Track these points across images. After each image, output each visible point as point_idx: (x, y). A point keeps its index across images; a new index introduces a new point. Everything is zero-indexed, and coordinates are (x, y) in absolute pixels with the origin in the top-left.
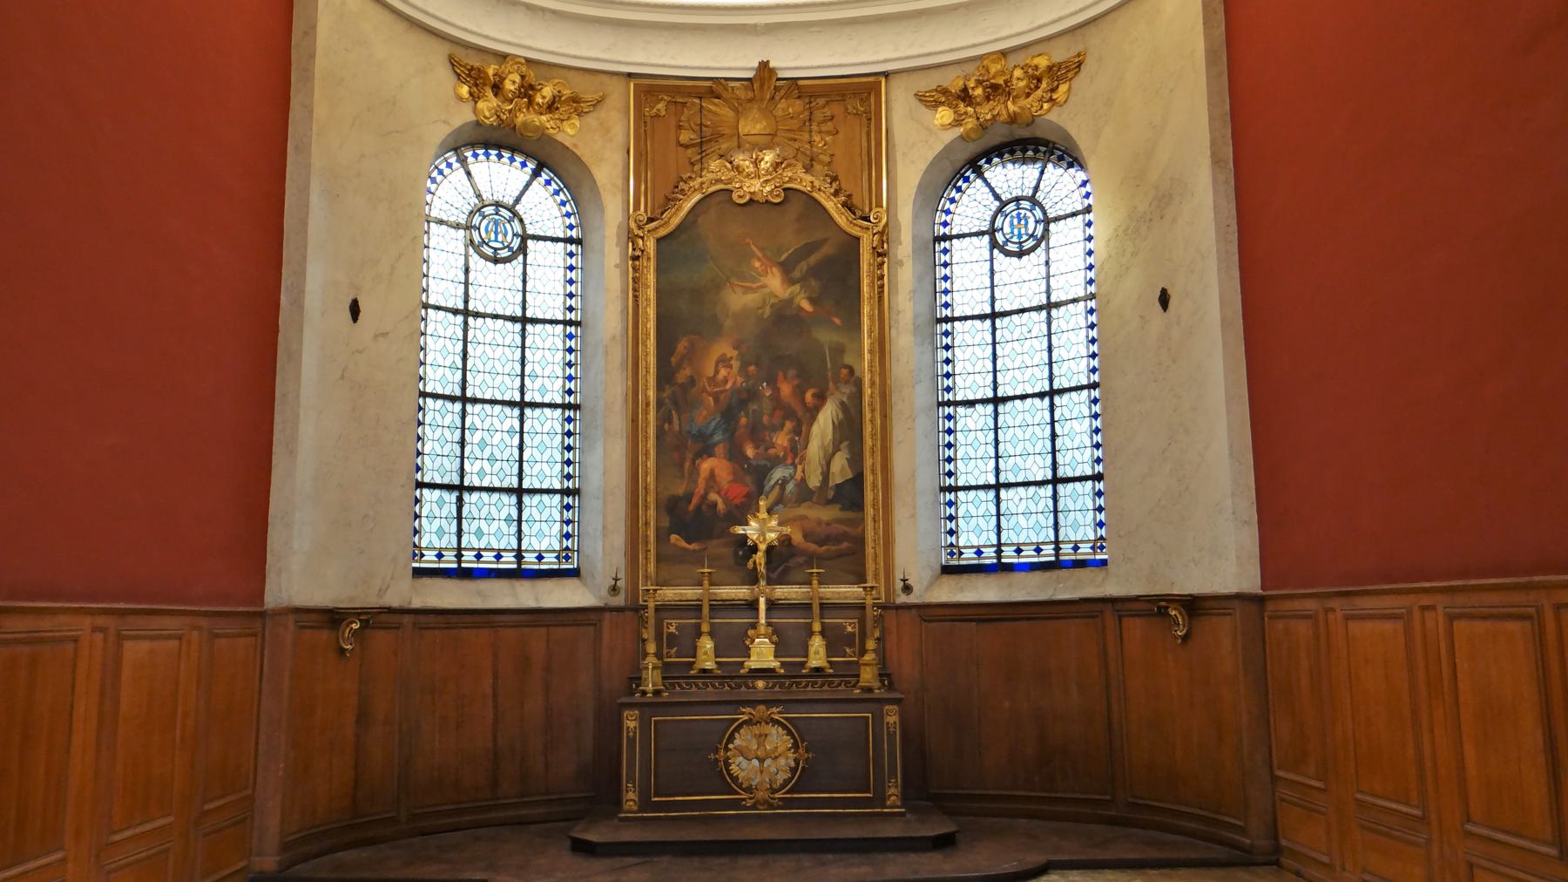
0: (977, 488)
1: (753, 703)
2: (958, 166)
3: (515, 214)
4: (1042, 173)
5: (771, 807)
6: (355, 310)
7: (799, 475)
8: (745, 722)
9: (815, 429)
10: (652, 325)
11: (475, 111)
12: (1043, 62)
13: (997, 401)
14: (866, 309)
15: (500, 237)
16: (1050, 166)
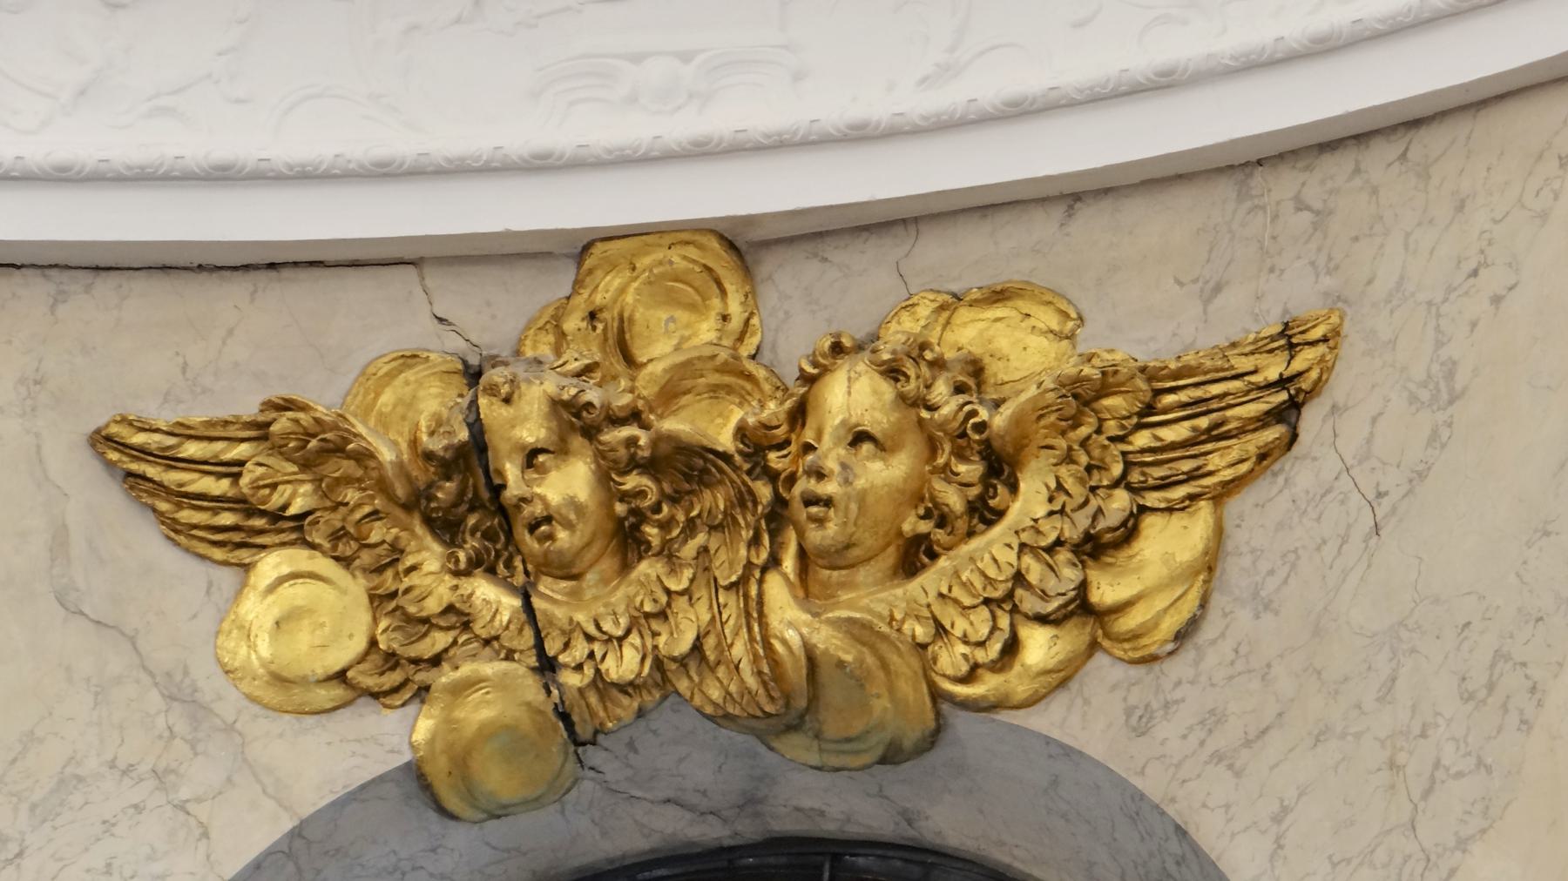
12: (1024, 354)
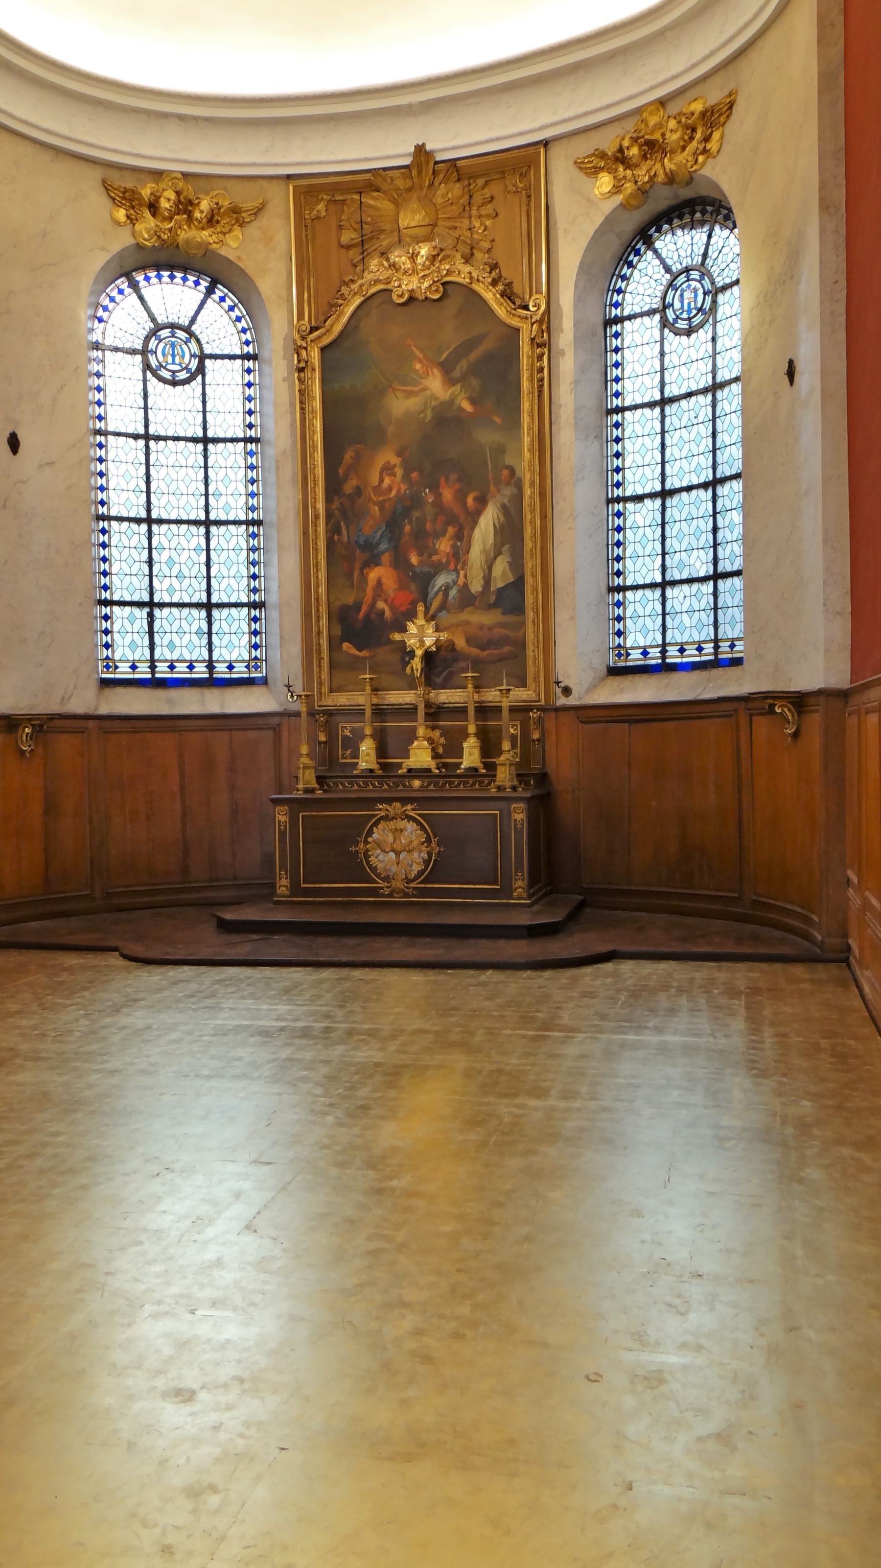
0: (644, 587)
1: (404, 801)
2: (627, 237)
3: (191, 334)
4: (710, 236)
5: (406, 895)
6: (14, 443)
7: (461, 581)
8: (382, 818)
9: (477, 534)
10: (318, 437)
11: (134, 234)
12: (697, 107)
13: (665, 494)
14: (526, 405)
15: (177, 360)
16: (717, 228)
